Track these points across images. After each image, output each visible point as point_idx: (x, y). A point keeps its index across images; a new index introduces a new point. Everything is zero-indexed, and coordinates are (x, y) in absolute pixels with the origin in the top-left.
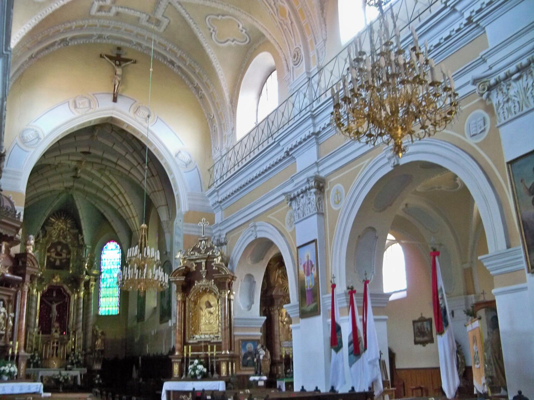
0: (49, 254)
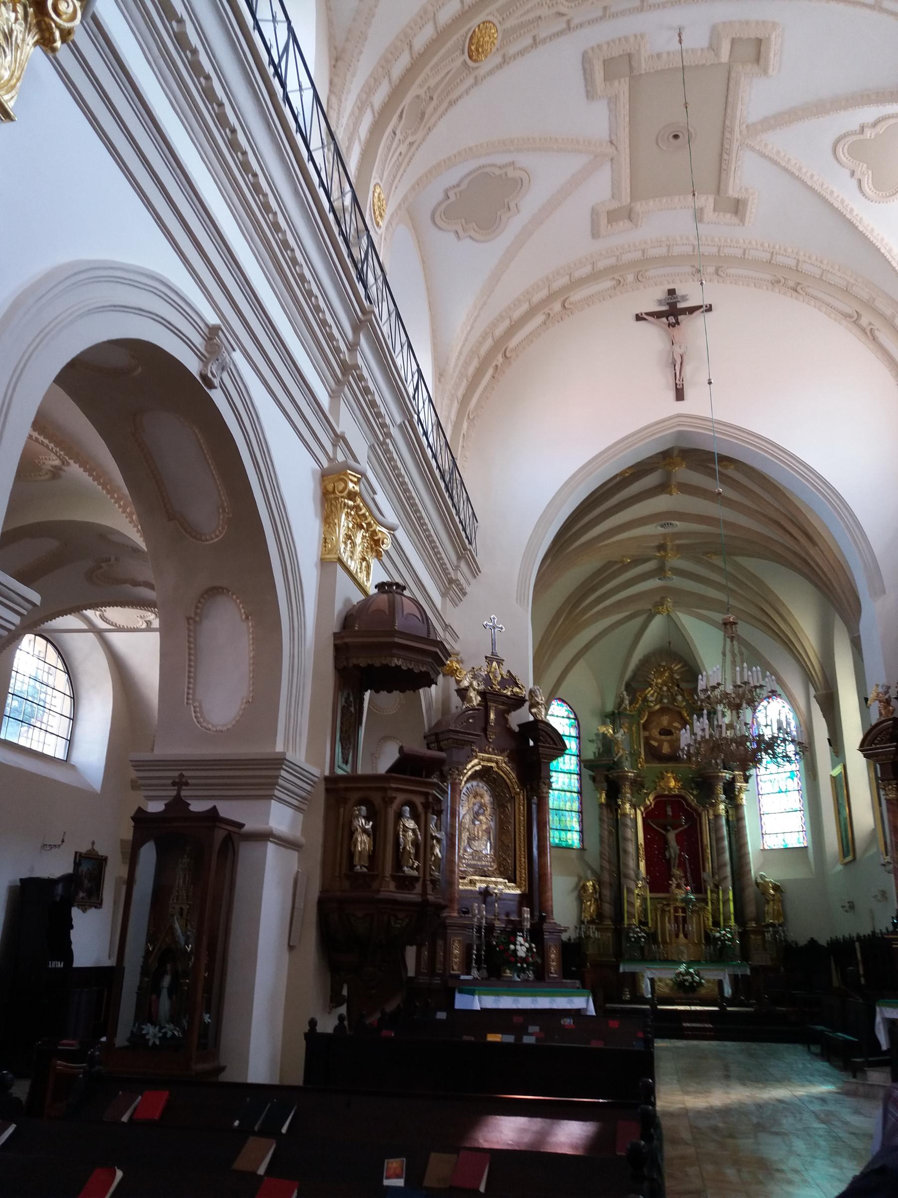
0: (647, 734)
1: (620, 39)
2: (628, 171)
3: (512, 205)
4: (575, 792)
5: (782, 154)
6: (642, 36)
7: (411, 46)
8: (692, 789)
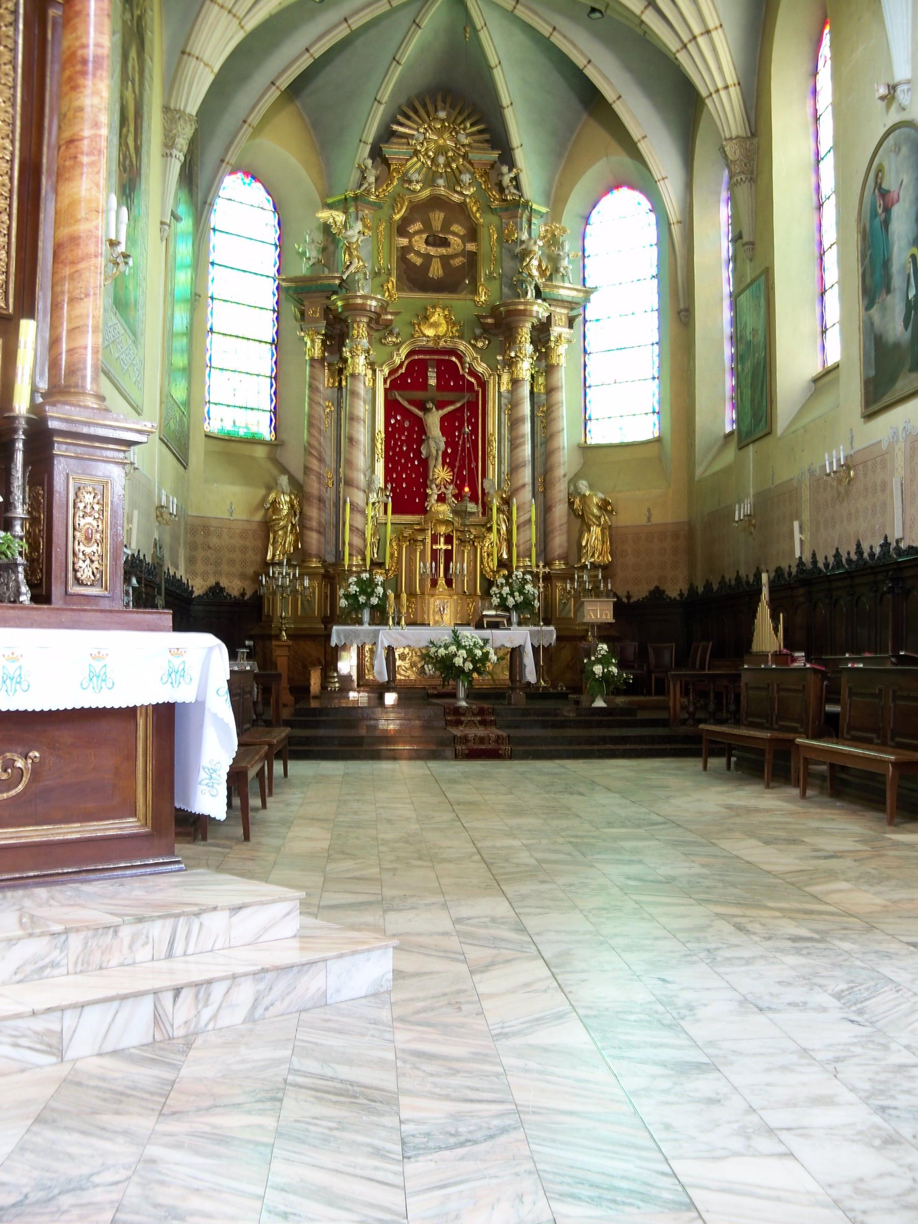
4: (266, 342)
8: (476, 340)
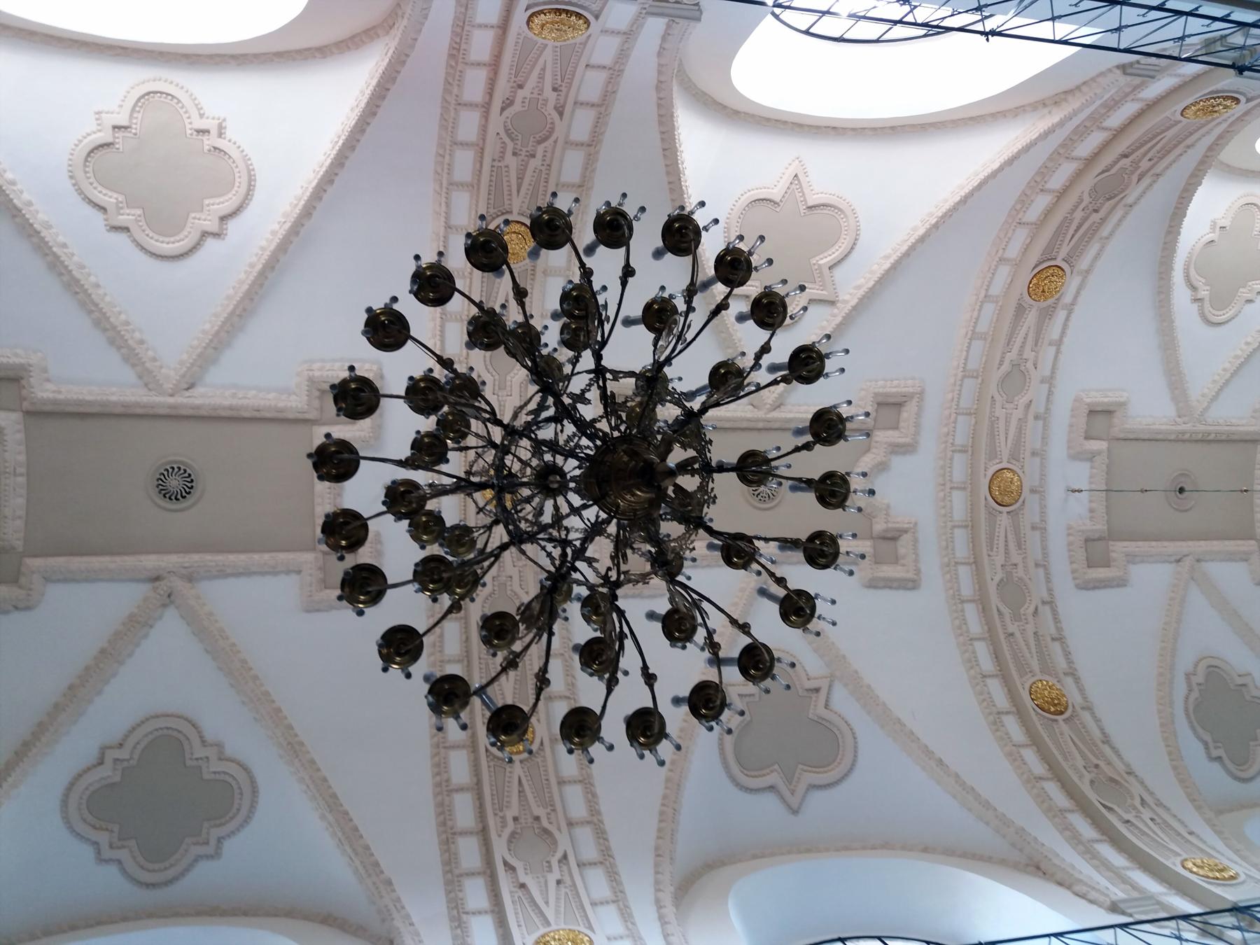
1: (1070, 551)
2: (1215, 543)
3: (1240, 681)
5: (1217, 378)
6: (1069, 528)
7: (1041, 778)
